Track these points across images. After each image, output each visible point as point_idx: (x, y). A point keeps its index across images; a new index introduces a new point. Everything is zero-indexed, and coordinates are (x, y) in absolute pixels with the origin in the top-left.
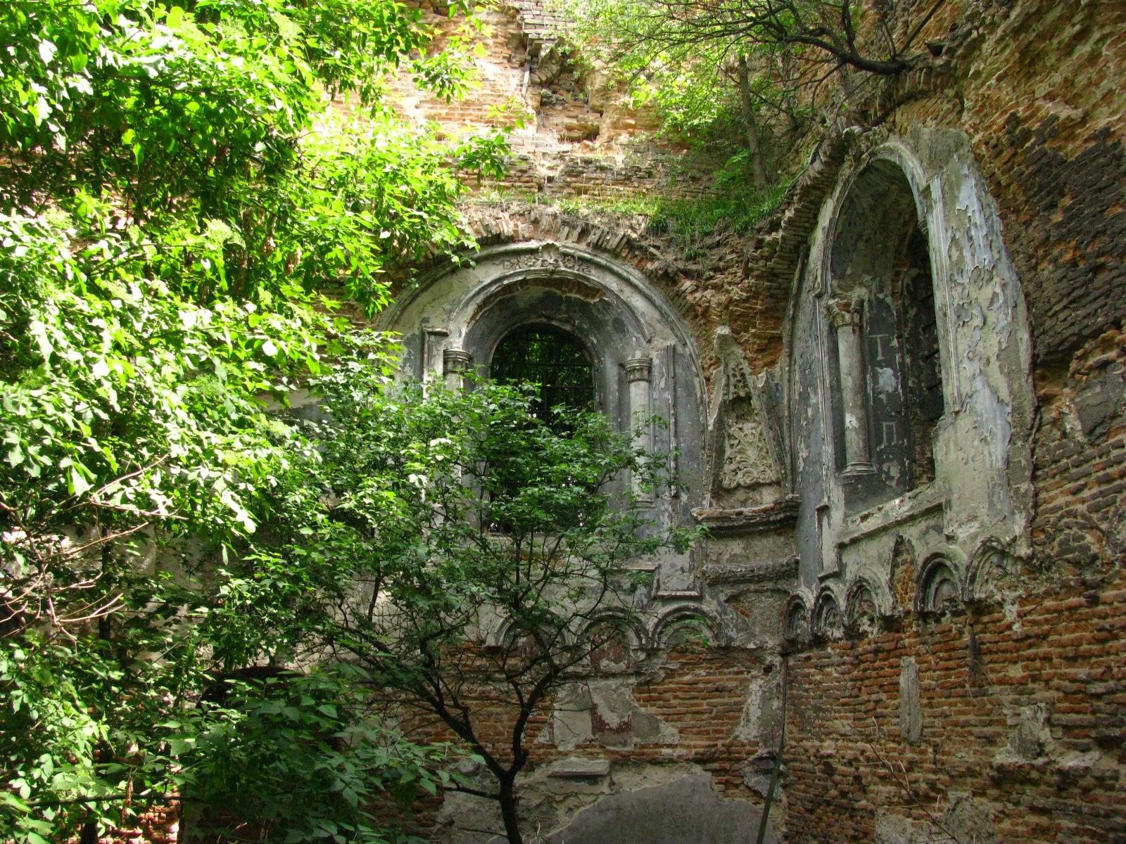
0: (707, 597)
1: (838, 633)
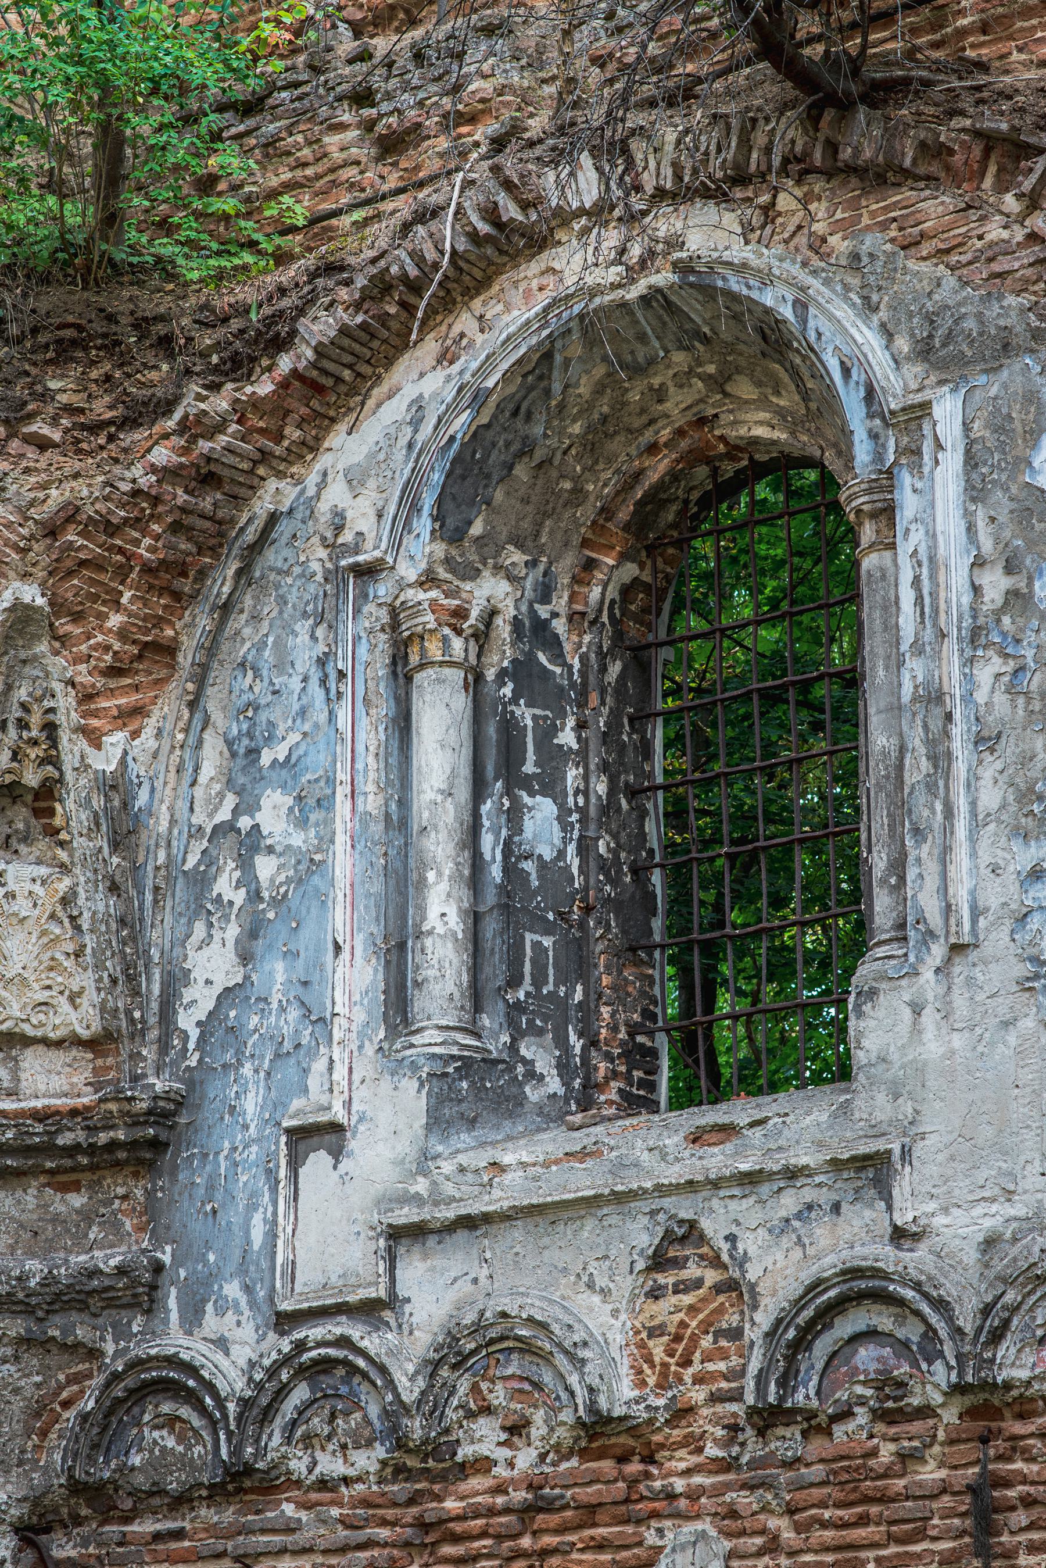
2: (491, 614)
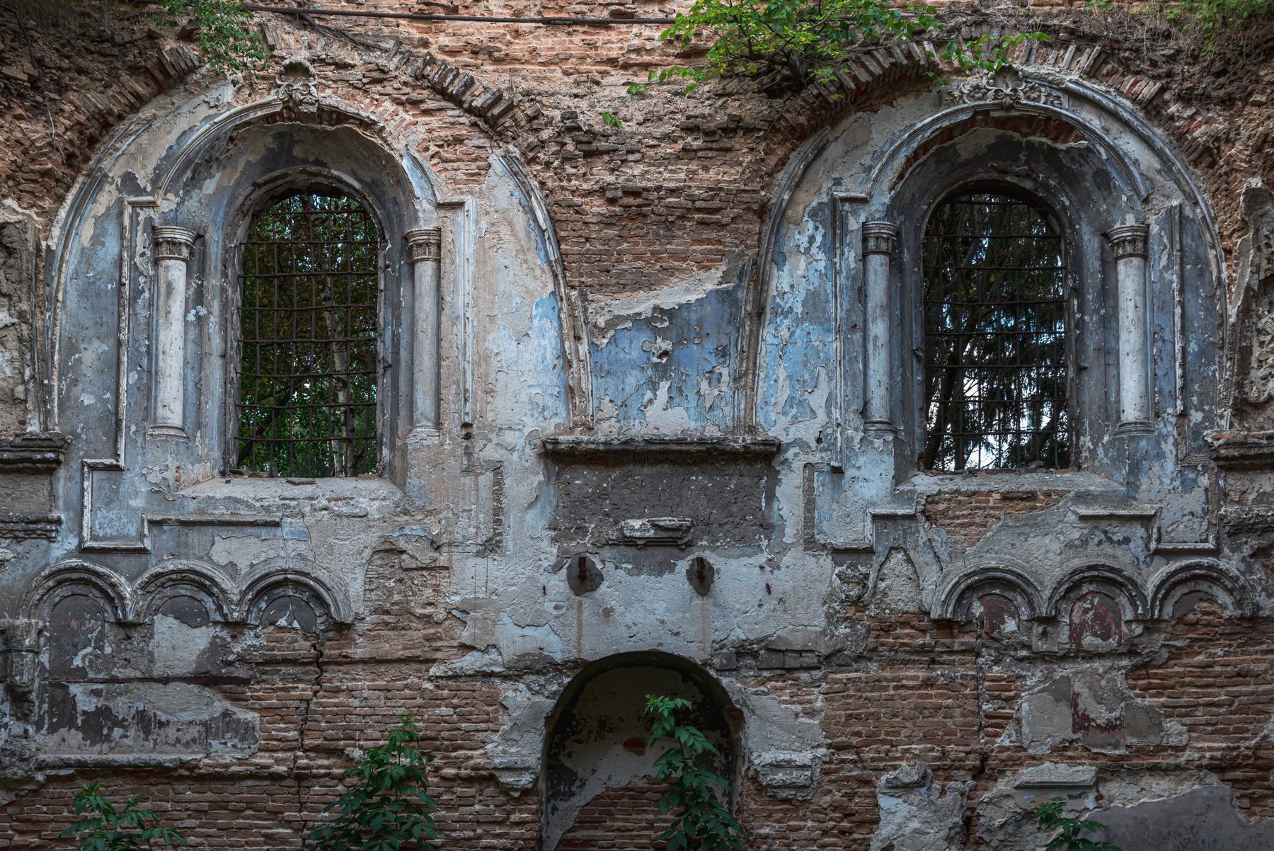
0: (1226, 550)
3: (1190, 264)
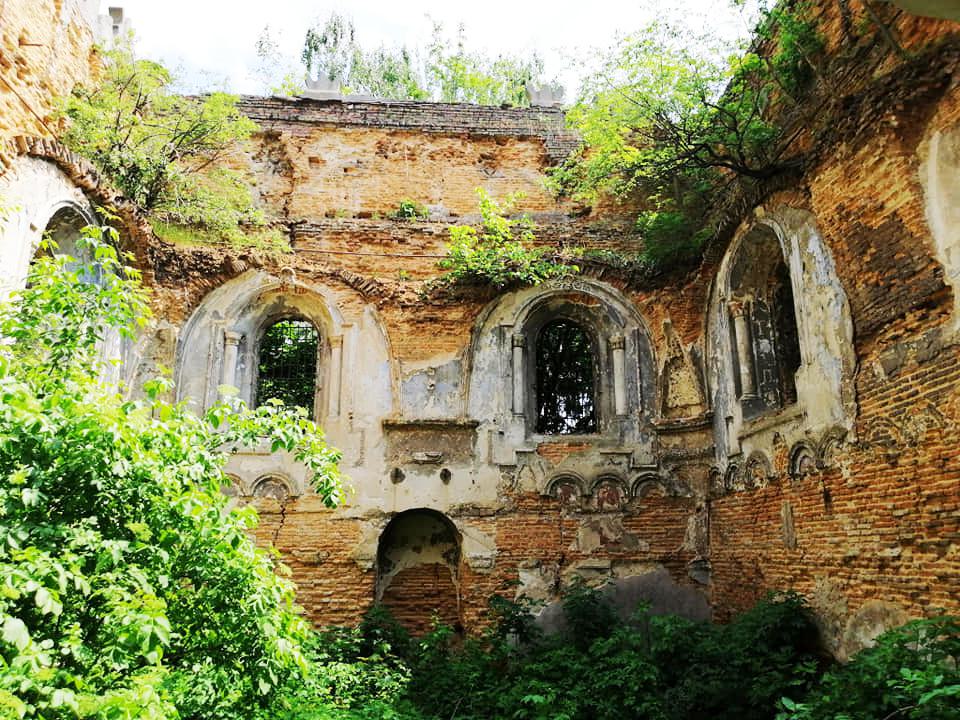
1: (741, 487)
2: (748, 303)
3: (644, 355)
